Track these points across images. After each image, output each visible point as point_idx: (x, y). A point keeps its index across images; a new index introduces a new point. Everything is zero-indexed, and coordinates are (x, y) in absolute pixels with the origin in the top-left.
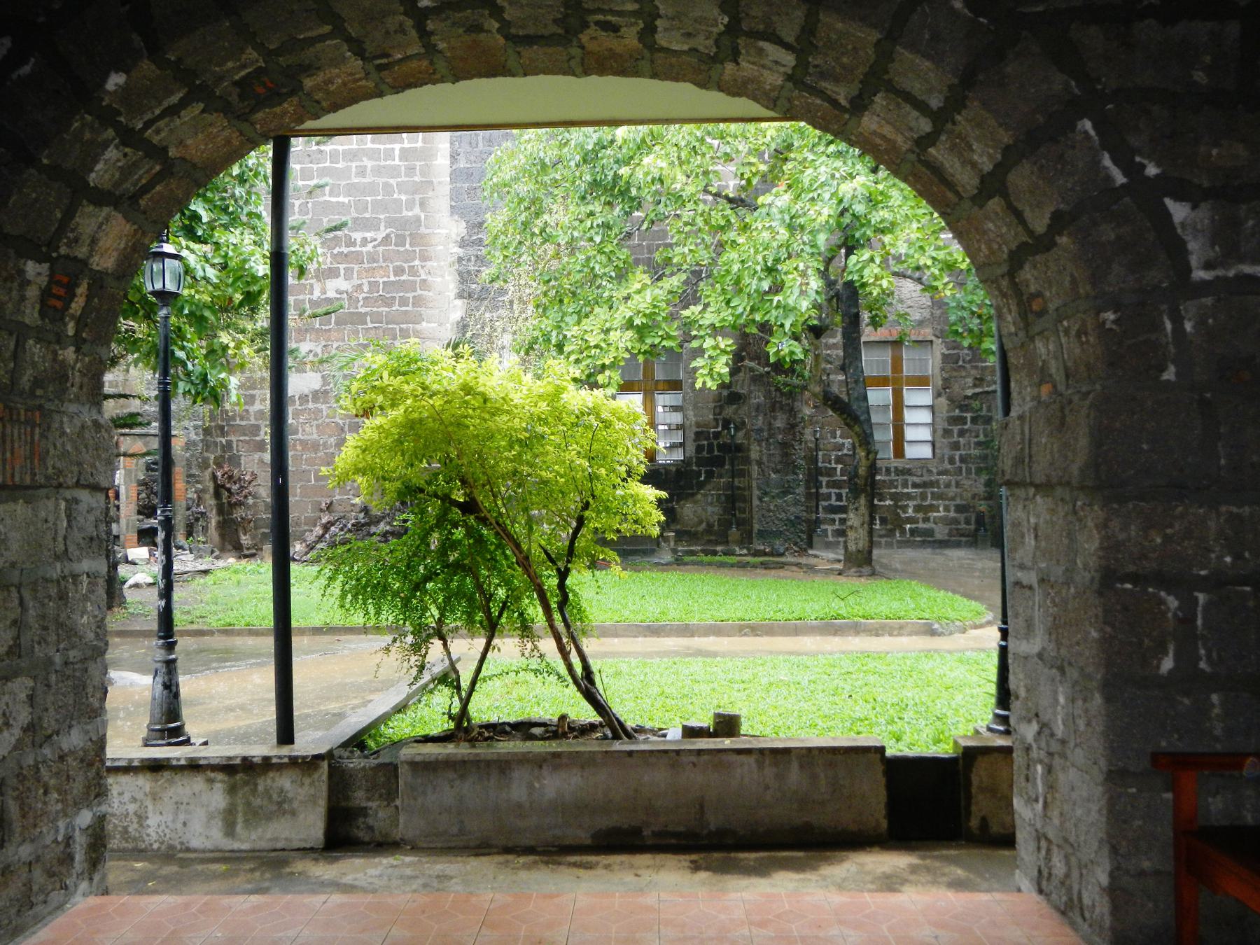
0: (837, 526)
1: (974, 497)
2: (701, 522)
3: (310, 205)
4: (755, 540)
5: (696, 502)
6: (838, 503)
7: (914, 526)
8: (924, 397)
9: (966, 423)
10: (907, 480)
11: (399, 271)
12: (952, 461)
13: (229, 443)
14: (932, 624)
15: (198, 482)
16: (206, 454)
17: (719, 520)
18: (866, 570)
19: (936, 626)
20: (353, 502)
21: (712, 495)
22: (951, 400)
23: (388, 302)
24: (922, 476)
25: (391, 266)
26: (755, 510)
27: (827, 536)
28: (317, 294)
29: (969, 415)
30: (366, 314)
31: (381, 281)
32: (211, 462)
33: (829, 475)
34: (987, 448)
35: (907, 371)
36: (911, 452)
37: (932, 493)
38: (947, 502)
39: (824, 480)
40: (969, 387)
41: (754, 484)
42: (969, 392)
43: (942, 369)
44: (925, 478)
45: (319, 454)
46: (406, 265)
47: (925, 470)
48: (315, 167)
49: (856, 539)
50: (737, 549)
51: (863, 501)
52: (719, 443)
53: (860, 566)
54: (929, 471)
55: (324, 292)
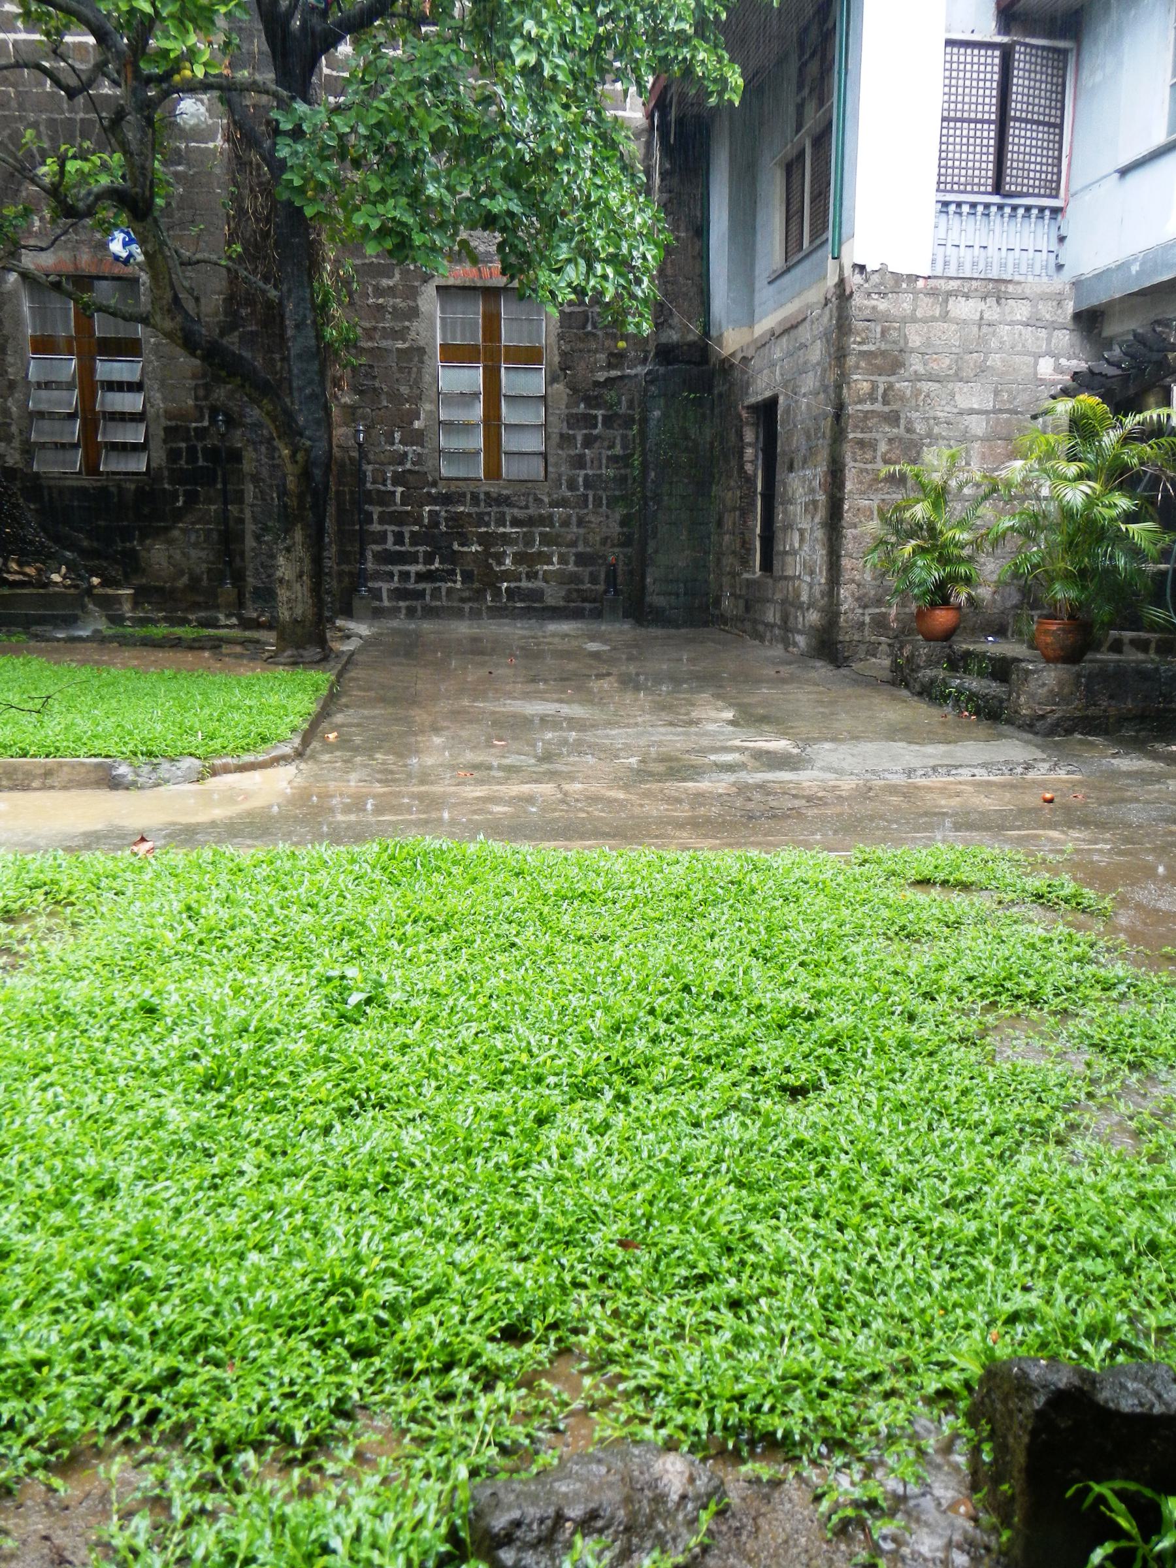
0: (395, 584)
1: (604, 541)
2: (181, 573)
4: (249, 603)
5: (170, 542)
6: (398, 548)
7: (513, 585)
8: (534, 382)
9: (595, 427)
10: (504, 514)
12: (572, 486)
14: (111, 767)
17: (209, 571)
18: (313, 652)
19: (123, 770)
21: (197, 531)
22: (574, 388)
24: (527, 507)
26: (249, 554)
27: (381, 600)
29: (600, 413)
33: (381, 503)
34: (627, 466)
35: (507, 337)
36: (508, 469)
37: (541, 534)
38: (563, 550)
39: (376, 511)
40: (602, 368)
41: (248, 515)
42: (601, 376)
43: (561, 337)
44: (530, 511)
47: (531, 499)
49: (289, 601)
50: (221, 617)
51: (298, 535)
52: (204, 449)
53: (299, 646)
54: (537, 500)
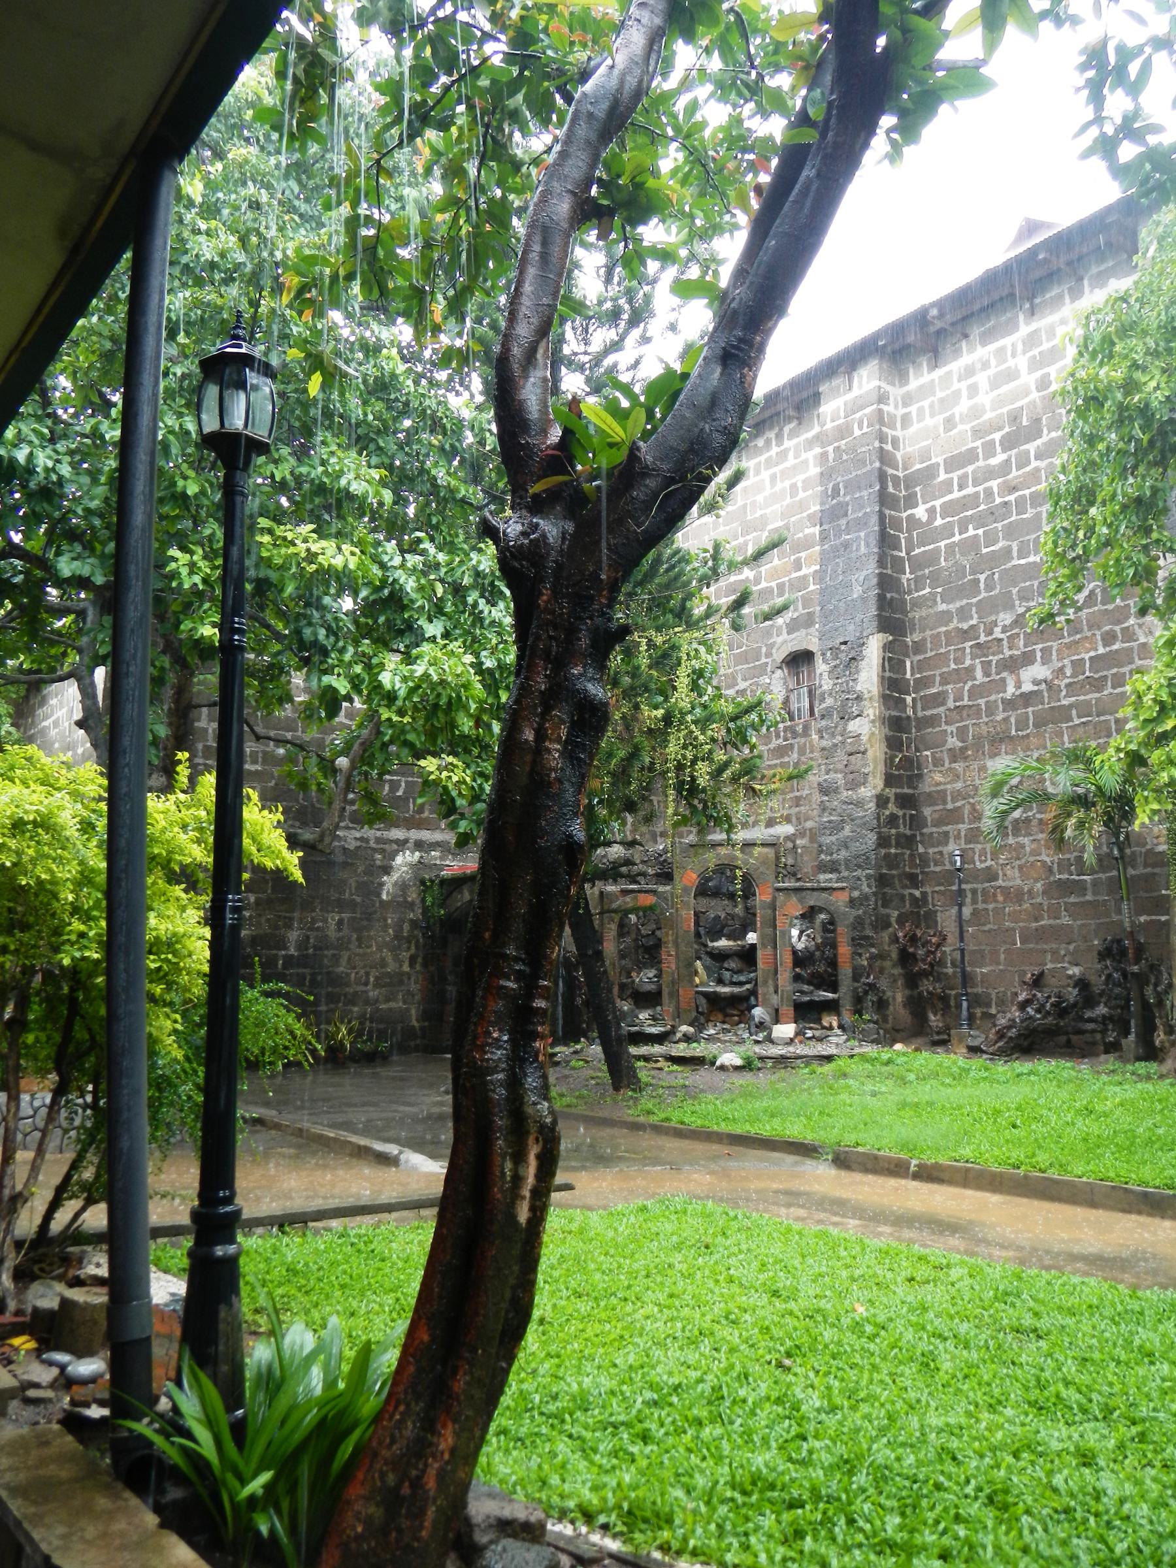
3: (996, 576)
11: (1109, 639)
13: (924, 894)
15: (872, 945)
16: (888, 911)
20: (1070, 972)
23: (1097, 684)
25: (1098, 633)
28: (1011, 690)
30: (1071, 706)
31: (1087, 657)
32: (893, 920)
45: (1026, 906)
46: (1117, 628)
48: (999, 525)
55: (1018, 685)
